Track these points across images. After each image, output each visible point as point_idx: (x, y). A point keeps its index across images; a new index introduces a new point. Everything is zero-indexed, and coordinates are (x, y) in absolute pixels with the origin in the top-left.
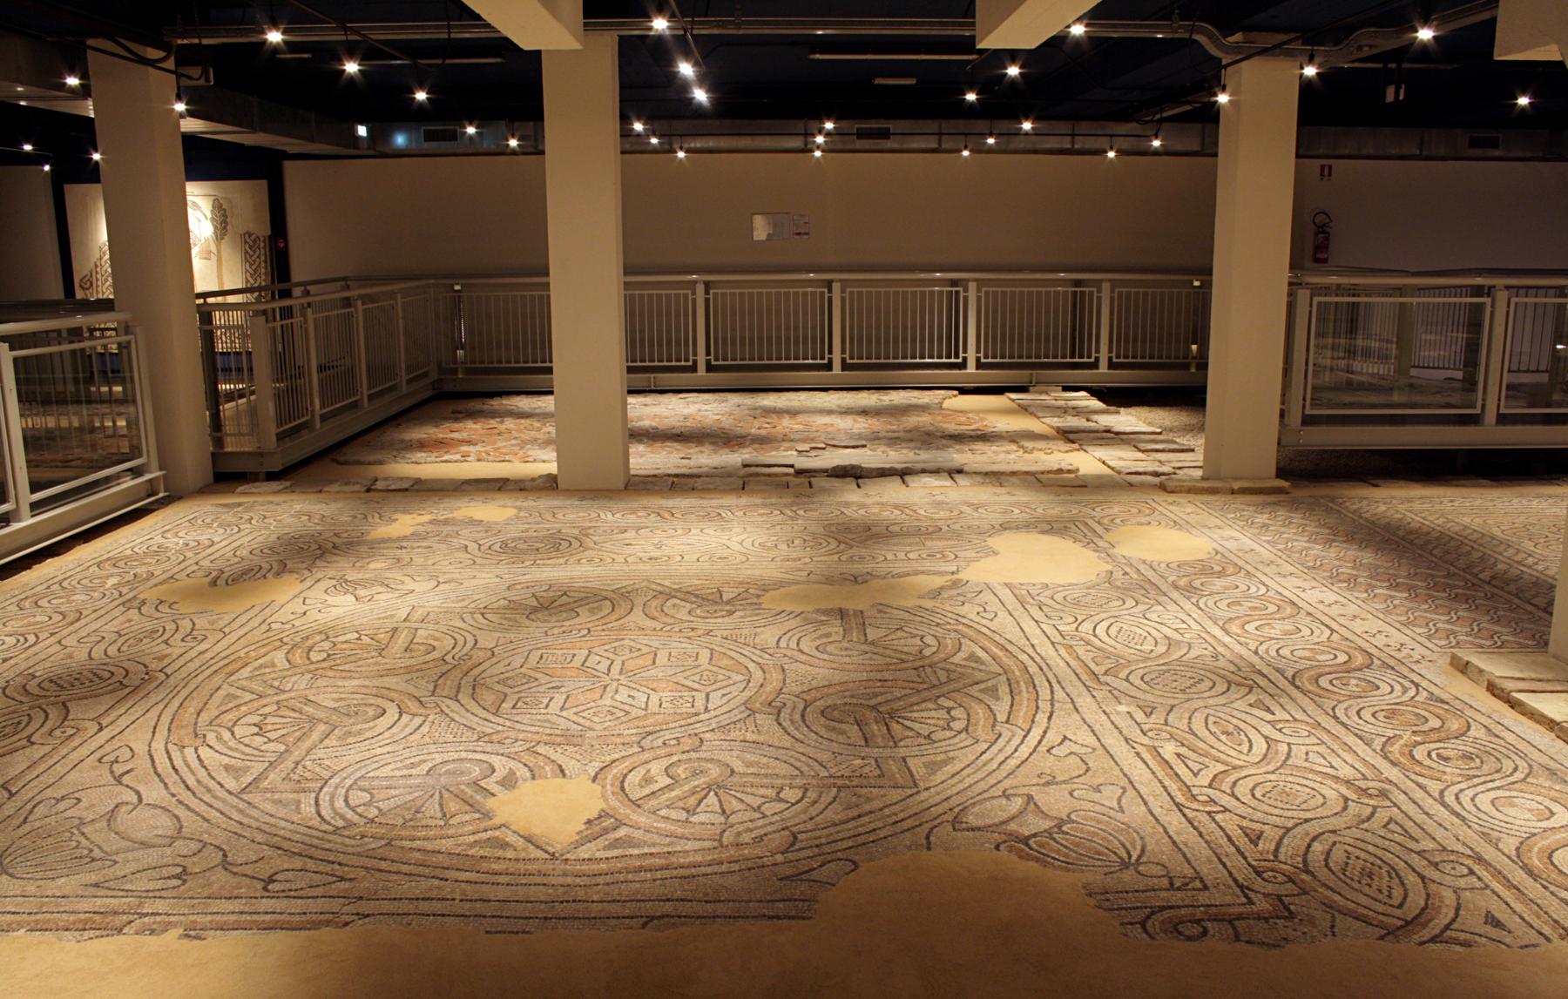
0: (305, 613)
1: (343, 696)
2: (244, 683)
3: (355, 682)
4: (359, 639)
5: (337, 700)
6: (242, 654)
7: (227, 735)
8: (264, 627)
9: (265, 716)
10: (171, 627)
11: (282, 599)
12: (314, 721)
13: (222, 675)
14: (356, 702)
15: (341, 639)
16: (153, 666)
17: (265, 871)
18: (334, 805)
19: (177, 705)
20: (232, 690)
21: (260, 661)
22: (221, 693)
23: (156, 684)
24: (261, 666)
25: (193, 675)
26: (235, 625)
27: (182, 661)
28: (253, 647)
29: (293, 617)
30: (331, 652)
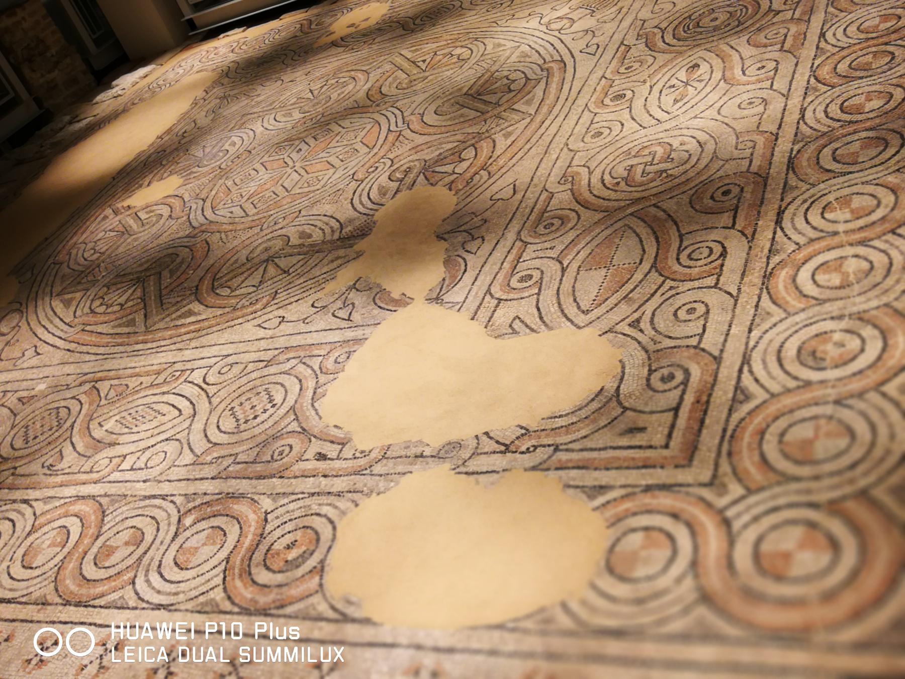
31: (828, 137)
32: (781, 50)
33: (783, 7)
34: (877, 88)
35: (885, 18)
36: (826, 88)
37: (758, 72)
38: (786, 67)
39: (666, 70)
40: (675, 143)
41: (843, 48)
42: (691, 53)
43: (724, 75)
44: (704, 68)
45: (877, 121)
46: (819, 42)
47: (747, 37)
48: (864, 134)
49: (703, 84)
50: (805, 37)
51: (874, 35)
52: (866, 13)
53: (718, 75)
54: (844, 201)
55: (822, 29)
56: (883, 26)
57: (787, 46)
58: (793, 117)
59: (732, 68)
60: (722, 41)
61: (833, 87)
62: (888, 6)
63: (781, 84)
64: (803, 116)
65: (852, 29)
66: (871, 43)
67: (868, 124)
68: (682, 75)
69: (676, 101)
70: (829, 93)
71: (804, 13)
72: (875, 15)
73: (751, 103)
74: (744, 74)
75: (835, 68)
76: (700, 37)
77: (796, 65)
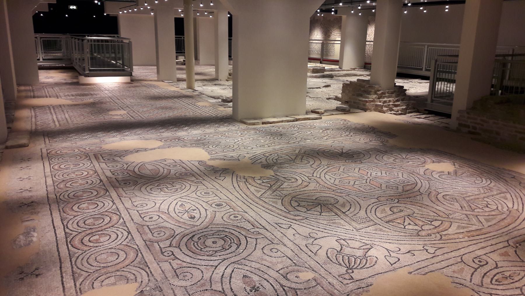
0: (409, 252)
1: (449, 205)
2: (477, 224)
3: (438, 208)
4: (409, 224)
5: (453, 205)
6: (466, 238)
7: (500, 208)
8: (438, 253)
9: (482, 209)
10: (487, 280)
11: (403, 272)
12: (468, 202)
13: (484, 231)
14: (448, 202)
15: (416, 227)
16: (511, 251)
17: (513, 179)
18: (485, 182)
19: (511, 226)
20: (484, 223)
21: (462, 231)
22: (490, 224)
23: (516, 239)
24: (464, 228)
25: (496, 237)
26: (451, 262)
27: (495, 247)
28: (457, 240)
29: (415, 253)
30: (429, 223)
31: (98, 196)
32: (148, 226)
33: (170, 249)
34: (85, 211)
35: (97, 241)
36: (110, 210)
37: (151, 216)
38: (137, 218)
39: (209, 216)
40: (162, 193)
41: (112, 226)
42: (205, 223)
43: (169, 213)
44: (186, 216)
45: (80, 201)
46: (128, 230)
47: (176, 233)
48: (83, 198)
49: (177, 211)
50: (139, 232)
51: (100, 233)
52: (111, 244)
53: (173, 214)
54: (81, 184)
55: (131, 235)
56: (97, 237)
57: (146, 228)
58: (117, 201)
59: (168, 218)
60: (191, 230)
61: (106, 211)
62: (99, 247)
63: (134, 213)
64: (112, 202)
65: (114, 236)
66: (100, 229)
67: (83, 200)
68: (197, 216)
69: (182, 205)
70: (107, 209)
71: (153, 245)
72: (105, 243)
73: (142, 205)
74: (159, 216)
75: (110, 218)
76: (212, 232)
77: (132, 219)
